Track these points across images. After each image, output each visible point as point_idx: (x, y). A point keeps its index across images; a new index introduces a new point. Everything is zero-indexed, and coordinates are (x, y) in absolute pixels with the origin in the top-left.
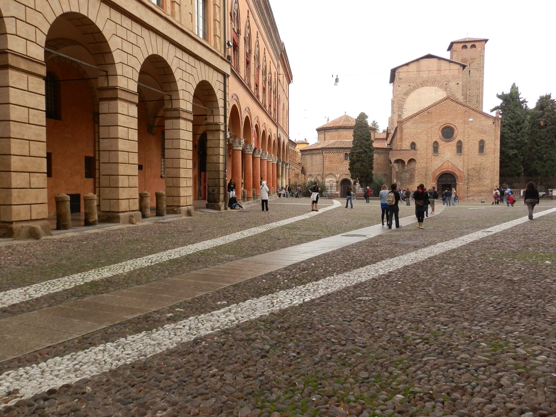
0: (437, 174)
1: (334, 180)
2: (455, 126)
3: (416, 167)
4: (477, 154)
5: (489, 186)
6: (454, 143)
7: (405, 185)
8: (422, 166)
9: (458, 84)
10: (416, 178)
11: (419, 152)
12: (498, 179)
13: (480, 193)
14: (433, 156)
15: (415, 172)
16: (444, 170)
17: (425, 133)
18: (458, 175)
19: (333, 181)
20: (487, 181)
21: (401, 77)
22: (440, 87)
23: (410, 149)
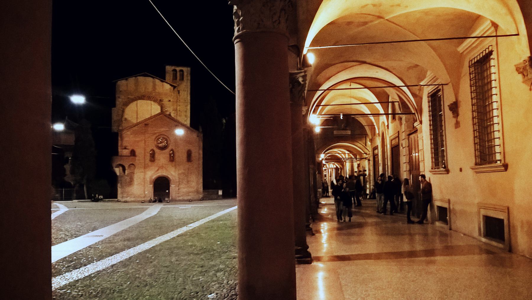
9: (170, 101)
11: (137, 158)
12: (202, 181)
13: (188, 193)
14: (150, 162)
17: (143, 142)
22: (155, 101)
23: (130, 155)
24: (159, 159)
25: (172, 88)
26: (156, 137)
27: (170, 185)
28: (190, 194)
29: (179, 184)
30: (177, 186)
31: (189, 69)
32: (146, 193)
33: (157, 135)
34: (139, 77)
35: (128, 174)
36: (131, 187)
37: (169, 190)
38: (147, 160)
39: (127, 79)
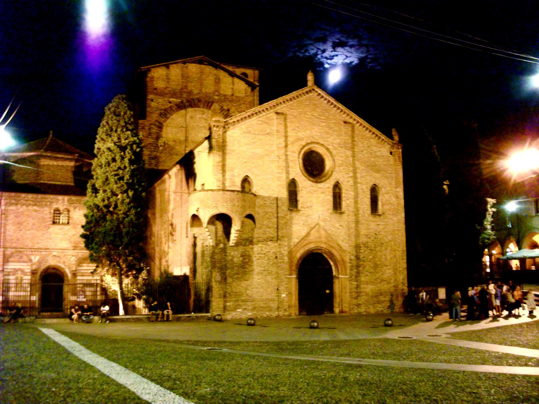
0: (298, 255)
1: (27, 268)
2: (328, 149)
3: (256, 236)
4: (369, 212)
5: (392, 281)
6: (327, 186)
7: (229, 280)
8: (268, 235)
10: (256, 262)
12: (405, 266)
15: (252, 248)
16: (312, 246)
18: (338, 257)
19: (22, 271)
20: (388, 271)
21: (156, 85)
24: (309, 204)
25: (249, 89)
26: (304, 147)
27: (334, 273)
28: (382, 298)
29: (358, 273)
30: (353, 277)
31: (257, 72)
32: (284, 295)
33: (304, 143)
34: (190, 64)
35: (237, 244)
36: (245, 280)
37: (331, 288)
38: (283, 208)
39: (168, 67)
